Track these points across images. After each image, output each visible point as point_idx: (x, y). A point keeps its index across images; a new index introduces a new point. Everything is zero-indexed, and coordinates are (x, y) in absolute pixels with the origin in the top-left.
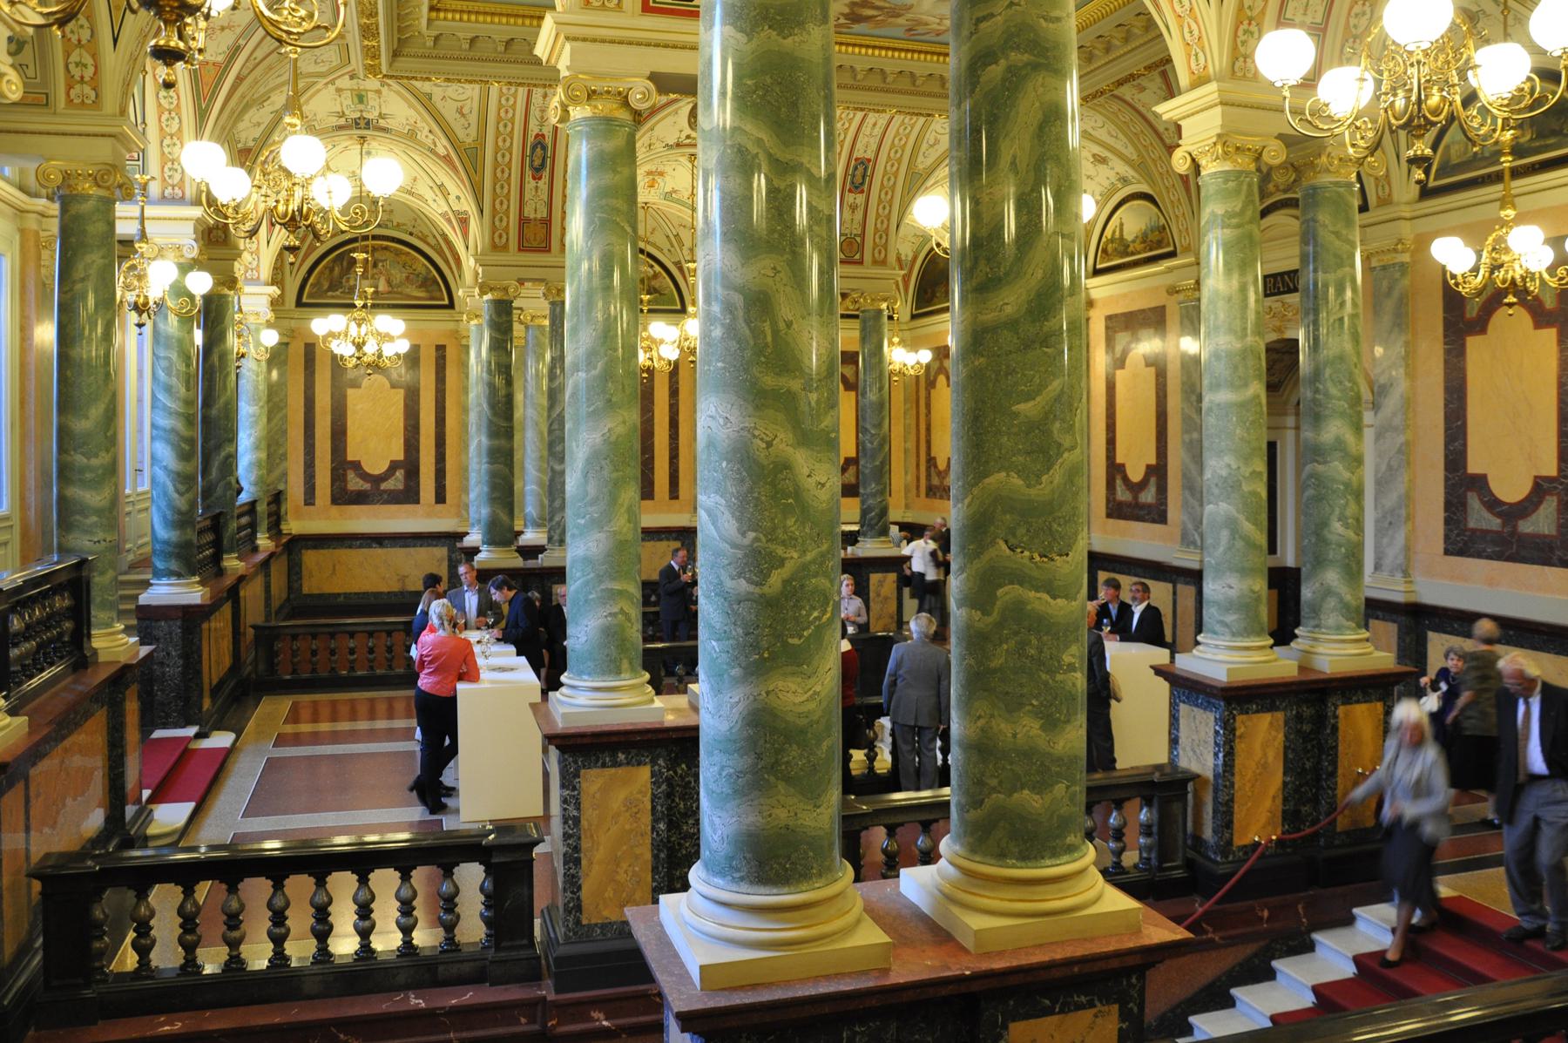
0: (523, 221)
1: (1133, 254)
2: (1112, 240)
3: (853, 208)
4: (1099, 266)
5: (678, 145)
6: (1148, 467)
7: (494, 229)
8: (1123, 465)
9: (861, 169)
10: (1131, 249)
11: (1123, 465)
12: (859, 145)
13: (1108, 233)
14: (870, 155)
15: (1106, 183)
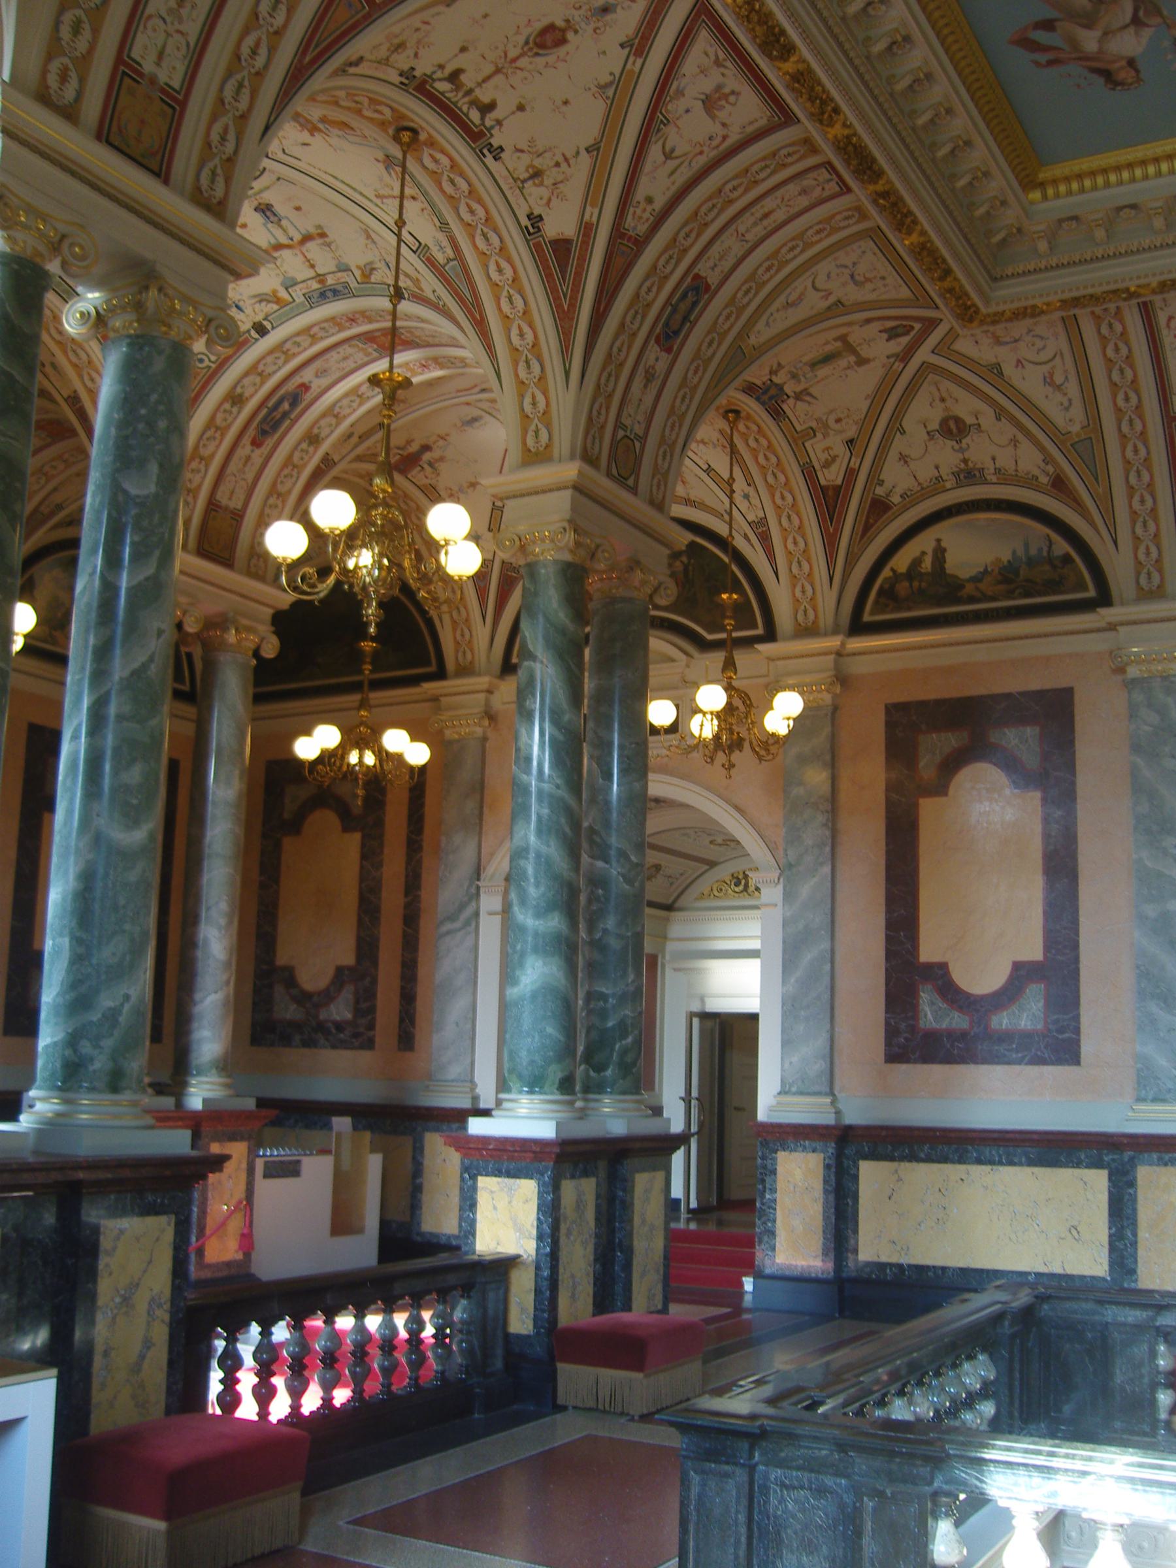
0: (125, 70)
1: (972, 600)
2: (913, 571)
3: (649, 377)
4: (867, 617)
5: (421, 87)
6: (1017, 966)
7: (54, 47)
8: (943, 966)
9: (691, 297)
10: (969, 589)
11: (943, 966)
12: (716, 249)
13: (901, 561)
14: (713, 279)
15: (926, 473)
